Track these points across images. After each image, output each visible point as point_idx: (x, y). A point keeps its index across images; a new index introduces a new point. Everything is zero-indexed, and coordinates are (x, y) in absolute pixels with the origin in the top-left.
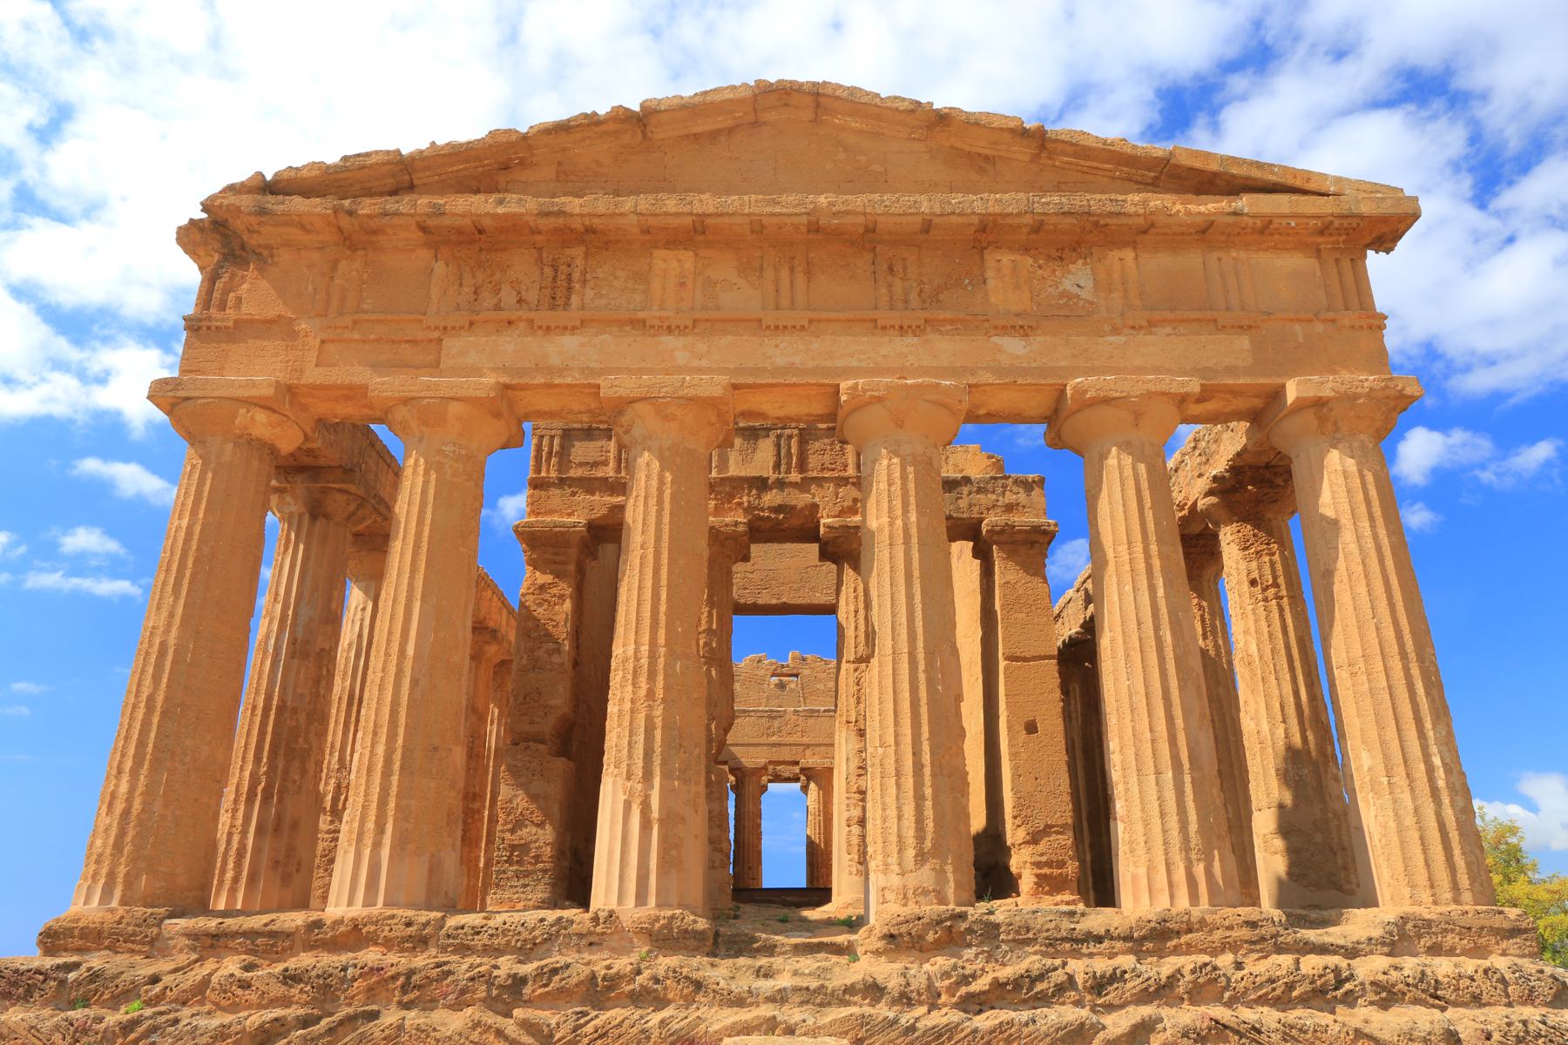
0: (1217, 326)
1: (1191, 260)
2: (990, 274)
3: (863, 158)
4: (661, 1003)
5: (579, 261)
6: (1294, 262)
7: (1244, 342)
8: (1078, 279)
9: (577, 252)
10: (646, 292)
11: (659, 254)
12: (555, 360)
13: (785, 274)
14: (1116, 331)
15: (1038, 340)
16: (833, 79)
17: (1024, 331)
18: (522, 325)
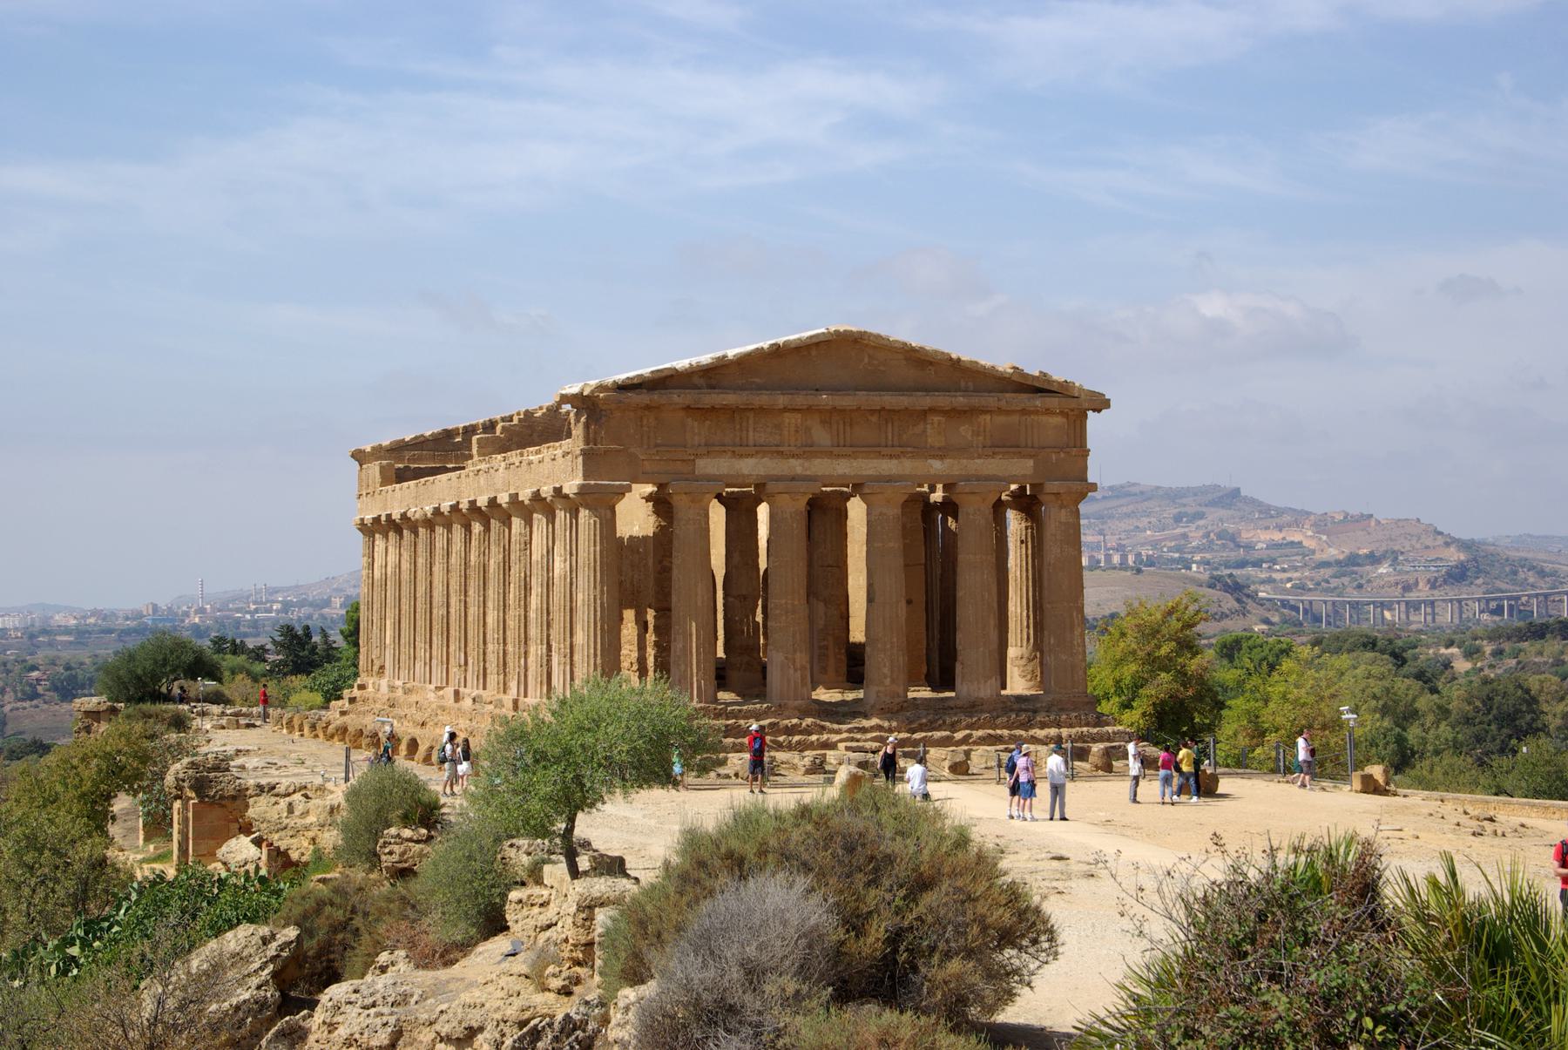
0: (1024, 457)
1: (1015, 418)
2: (928, 426)
3: (875, 362)
4: (810, 734)
5: (751, 422)
6: (1057, 420)
7: (1031, 463)
8: (965, 431)
9: (751, 415)
10: (780, 435)
11: (787, 414)
12: (746, 472)
13: (841, 426)
14: (979, 457)
15: (948, 461)
16: (868, 330)
17: (941, 458)
18: (730, 454)
